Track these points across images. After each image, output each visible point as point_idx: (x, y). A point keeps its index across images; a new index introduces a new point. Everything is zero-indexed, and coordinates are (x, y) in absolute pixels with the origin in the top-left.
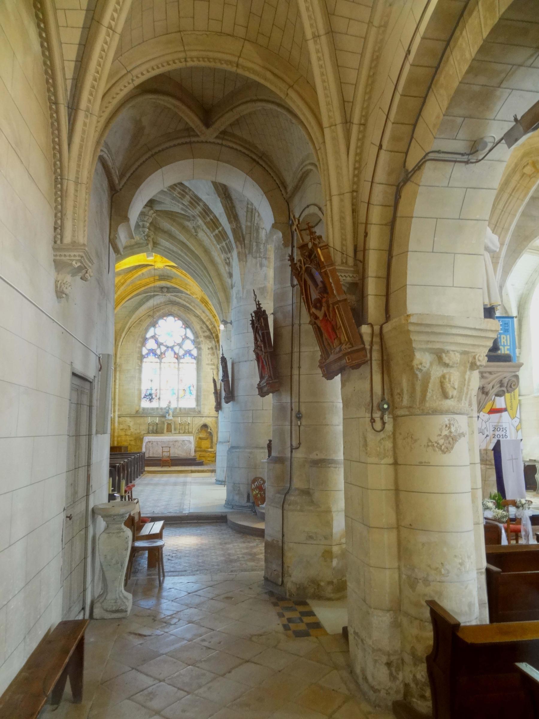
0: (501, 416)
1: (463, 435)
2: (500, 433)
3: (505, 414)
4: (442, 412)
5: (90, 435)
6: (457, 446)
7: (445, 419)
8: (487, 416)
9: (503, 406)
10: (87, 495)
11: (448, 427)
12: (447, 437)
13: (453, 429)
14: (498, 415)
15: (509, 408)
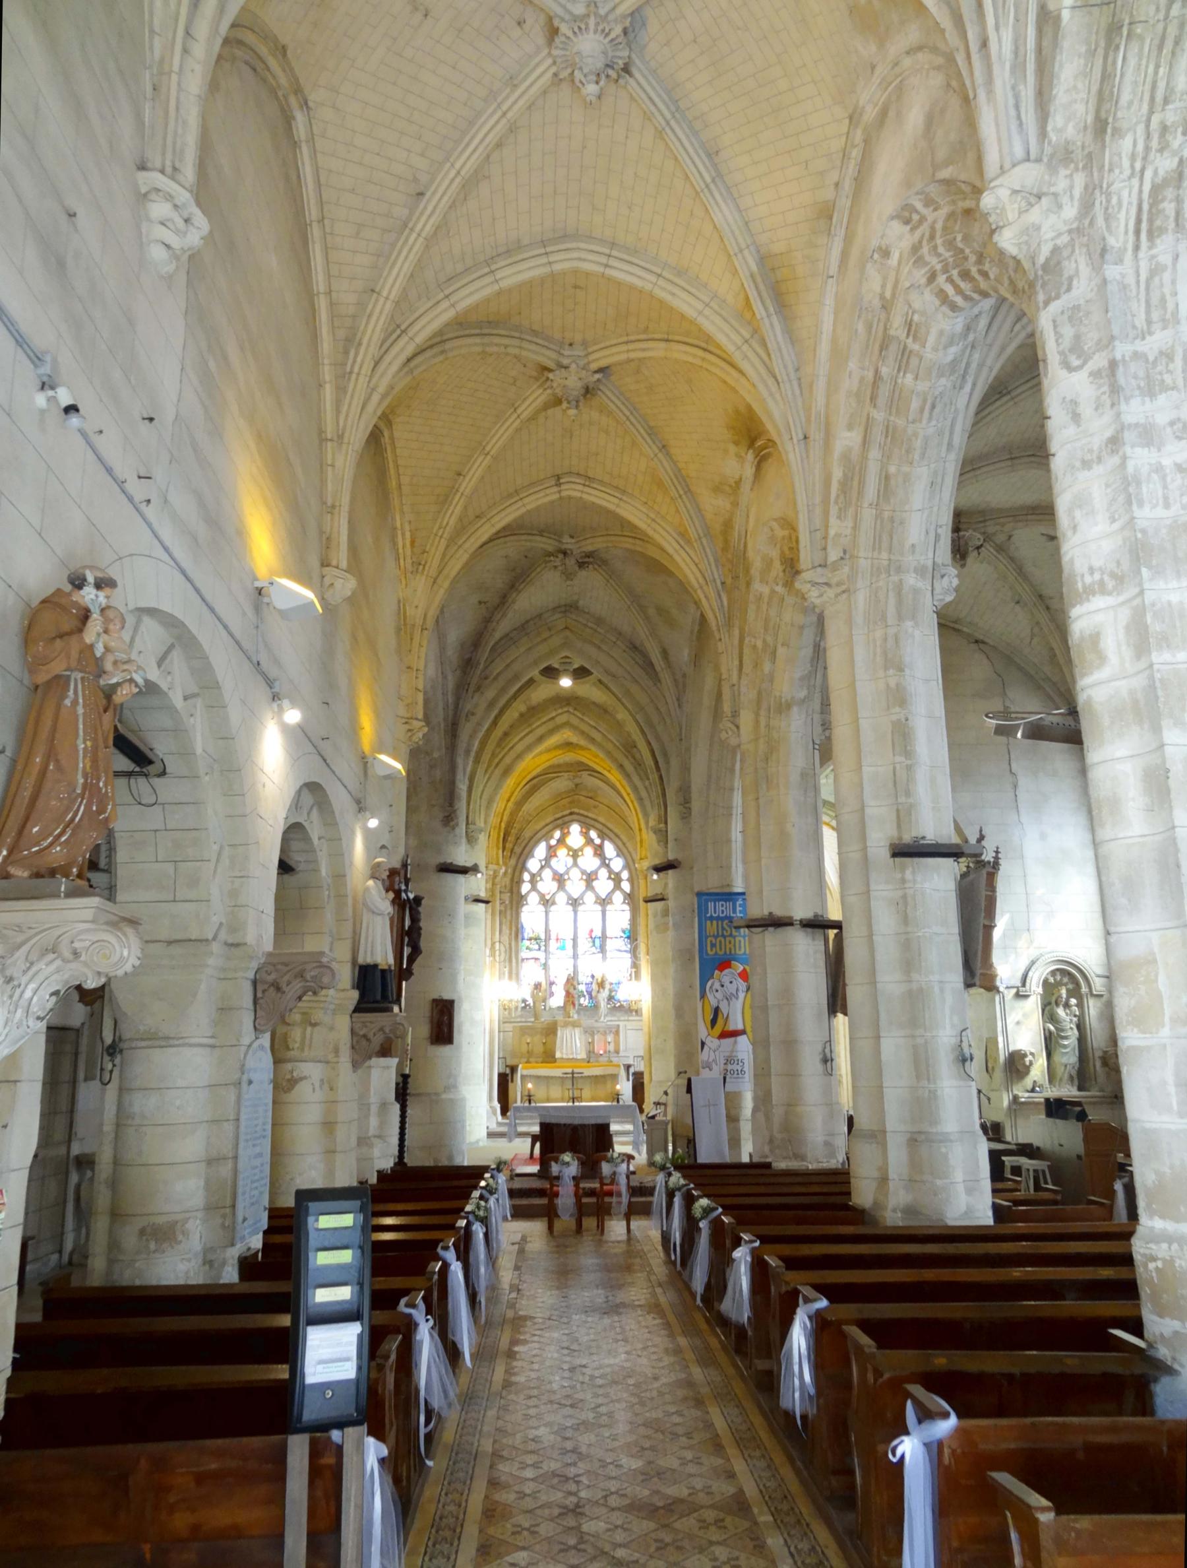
0: (735, 1042)
1: (305, 1078)
2: (735, 1067)
3: (743, 1040)
4: (290, 1061)
5: (74, 1082)
6: (297, 1087)
7: (289, 1066)
8: (716, 1042)
9: (740, 1027)
10: (69, 1141)
11: (292, 1072)
12: (289, 1080)
13: (295, 1074)
14: (732, 1039)
15: (749, 1030)
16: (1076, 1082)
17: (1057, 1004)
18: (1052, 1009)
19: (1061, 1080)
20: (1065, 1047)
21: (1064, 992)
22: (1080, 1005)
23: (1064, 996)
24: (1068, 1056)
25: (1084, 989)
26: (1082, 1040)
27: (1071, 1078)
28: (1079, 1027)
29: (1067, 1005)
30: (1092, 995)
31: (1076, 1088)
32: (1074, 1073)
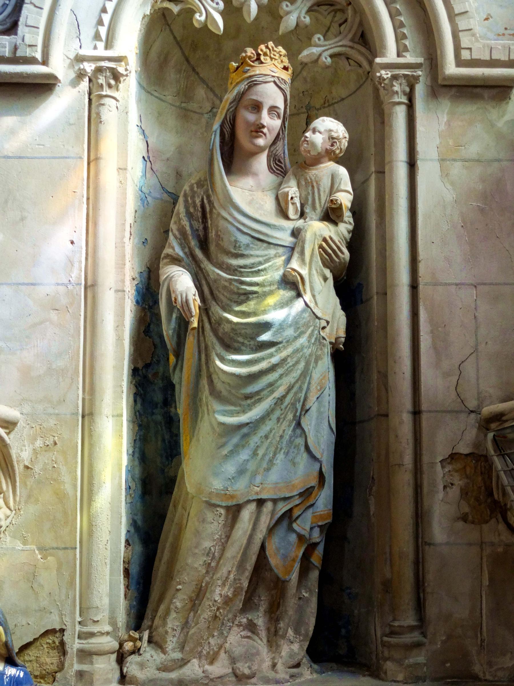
16: (304, 604)
17: (233, 155)
18: (207, 182)
19: (199, 594)
20: (242, 391)
21: (272, 77)
22: (363, 157)
23: (272, 96)
24: (259, 461)
25: (394, 49)
26: (353, 360)
27: (262, 583)
28: (352, 283)
29: (293, 161)
30: (447, 89)
31: (293, 647)
32: (284, 554)
